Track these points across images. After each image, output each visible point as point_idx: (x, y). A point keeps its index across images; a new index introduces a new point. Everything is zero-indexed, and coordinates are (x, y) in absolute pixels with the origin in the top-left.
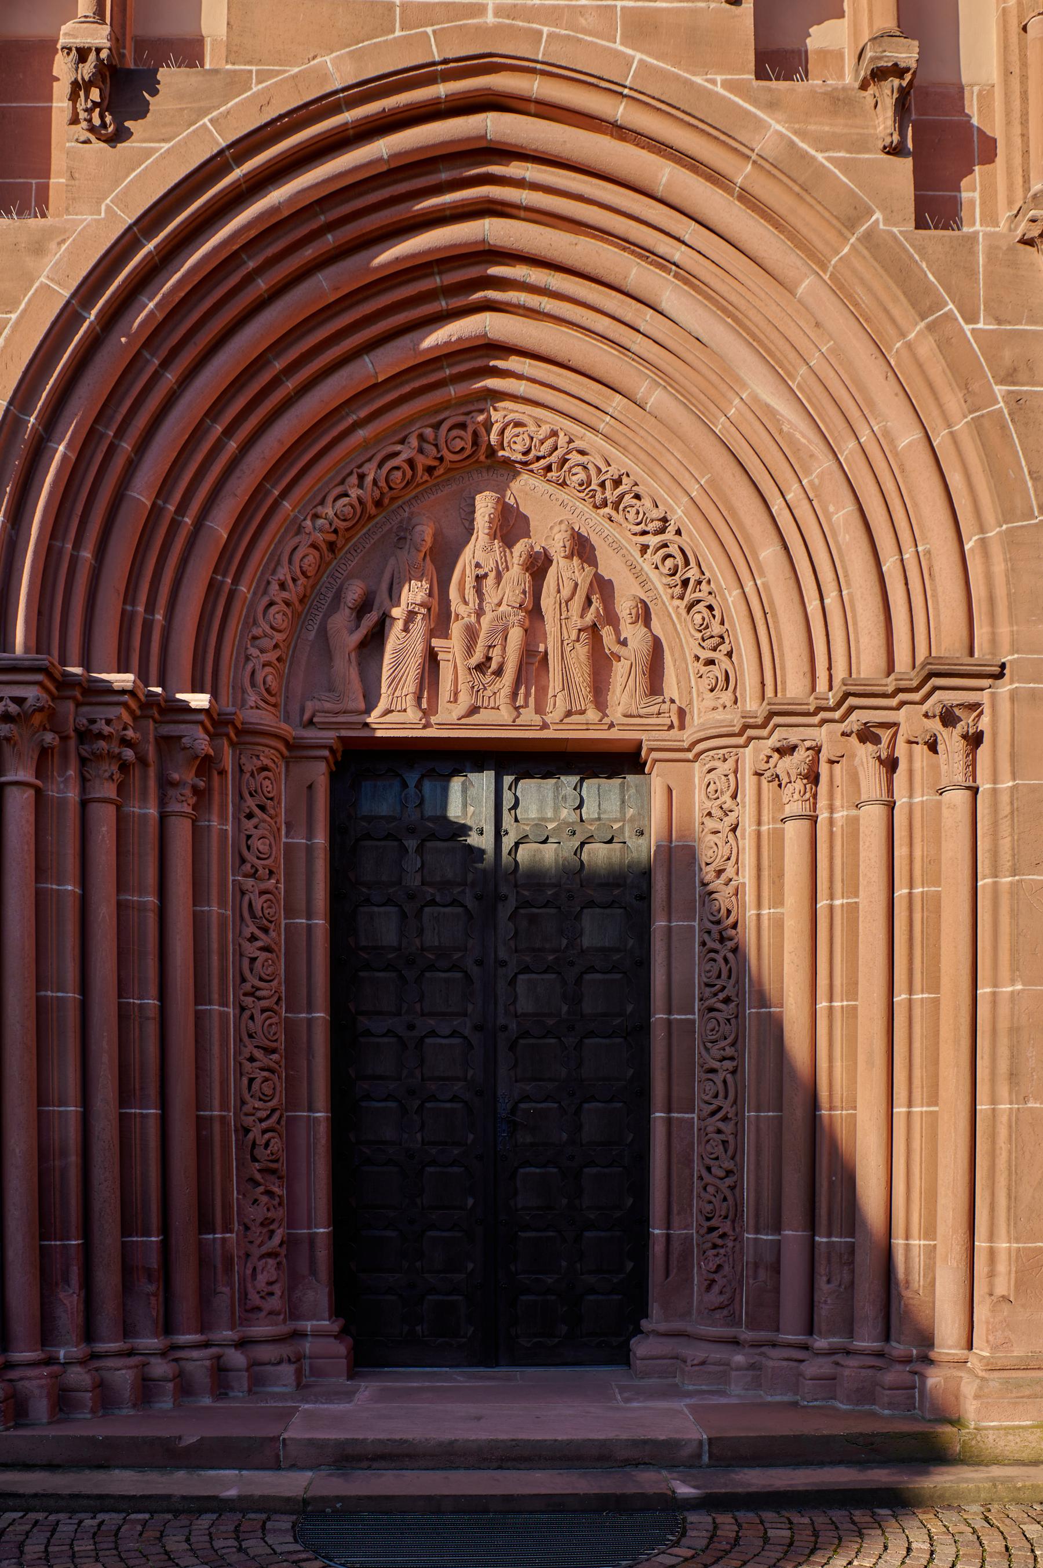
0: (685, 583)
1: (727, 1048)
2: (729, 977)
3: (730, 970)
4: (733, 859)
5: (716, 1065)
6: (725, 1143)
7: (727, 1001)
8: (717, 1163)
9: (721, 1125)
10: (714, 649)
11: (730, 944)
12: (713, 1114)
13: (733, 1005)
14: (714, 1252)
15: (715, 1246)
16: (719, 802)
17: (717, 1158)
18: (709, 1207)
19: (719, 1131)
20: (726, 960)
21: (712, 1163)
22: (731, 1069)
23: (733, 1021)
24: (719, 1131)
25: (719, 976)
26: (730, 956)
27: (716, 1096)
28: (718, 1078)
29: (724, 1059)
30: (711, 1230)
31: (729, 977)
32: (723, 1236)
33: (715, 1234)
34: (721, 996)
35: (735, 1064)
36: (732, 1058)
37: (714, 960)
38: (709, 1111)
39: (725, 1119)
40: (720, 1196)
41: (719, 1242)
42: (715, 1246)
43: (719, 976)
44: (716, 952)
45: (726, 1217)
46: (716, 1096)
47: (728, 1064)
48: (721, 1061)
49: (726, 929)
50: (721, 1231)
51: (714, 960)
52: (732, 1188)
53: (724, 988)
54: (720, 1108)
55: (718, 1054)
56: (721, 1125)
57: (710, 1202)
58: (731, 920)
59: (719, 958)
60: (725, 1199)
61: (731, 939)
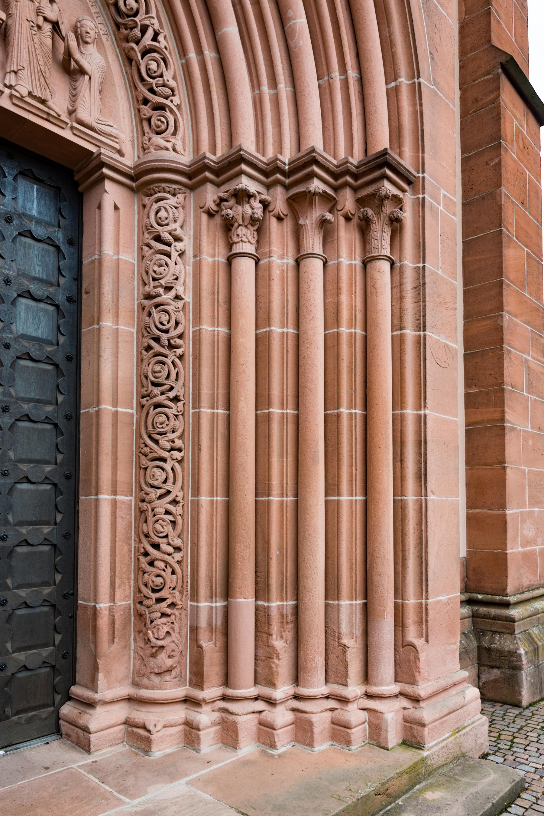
0: (144, 29)
1: (176, 440)
2: (177, 380)
3: (177, 374)
4: (181, 280)
5: (165, 454)
6: (174, 523)
7: (176, 399)
8: (165, 540)
9: (171, 508)
10: (167, 98)
11: (179, 351)
12: (160, 497)
13: (180, 404)
14: (164, 620)
15: (163, 615)
16: (167, 228)
17: (166, 536)
18: (159, 580)
19: (168, 512)
20: (175, 365)
21: (161, 541)
22: (179, 459)
23: (181, 417)
24: (168, 512)
25: (168, 377)
26: (177, 361)
27: (165, 481)
28: (167, 467)
29: (172, 449)
30: (160, 600)
31: (177, 380)
32: (173, 605)
33: (164, 604)
34: (171, 394)
35: (182, 454)
36: (180, 450)
37: (164, 363)
38: (158, 495)
39: (175, 502)
40: (169, 570)
41: (169, 611)
42: (163, 615)
43: (168, 377)
44: (166, 357)
45: (174, 589)
46: (165, 481)
47: (177, 455)
48: (169, 451)
49: (173, 338)
50: (169, 601)
51: (164, 363)
52: (179, 562)
53: (172, 388)
54: (169, 492)
55: (168, 446)
56: (171, 508)
57: (158, 576)
58: (180, 330)
59: (169, 361)
60: (173, 572)
61: (178, 347)
